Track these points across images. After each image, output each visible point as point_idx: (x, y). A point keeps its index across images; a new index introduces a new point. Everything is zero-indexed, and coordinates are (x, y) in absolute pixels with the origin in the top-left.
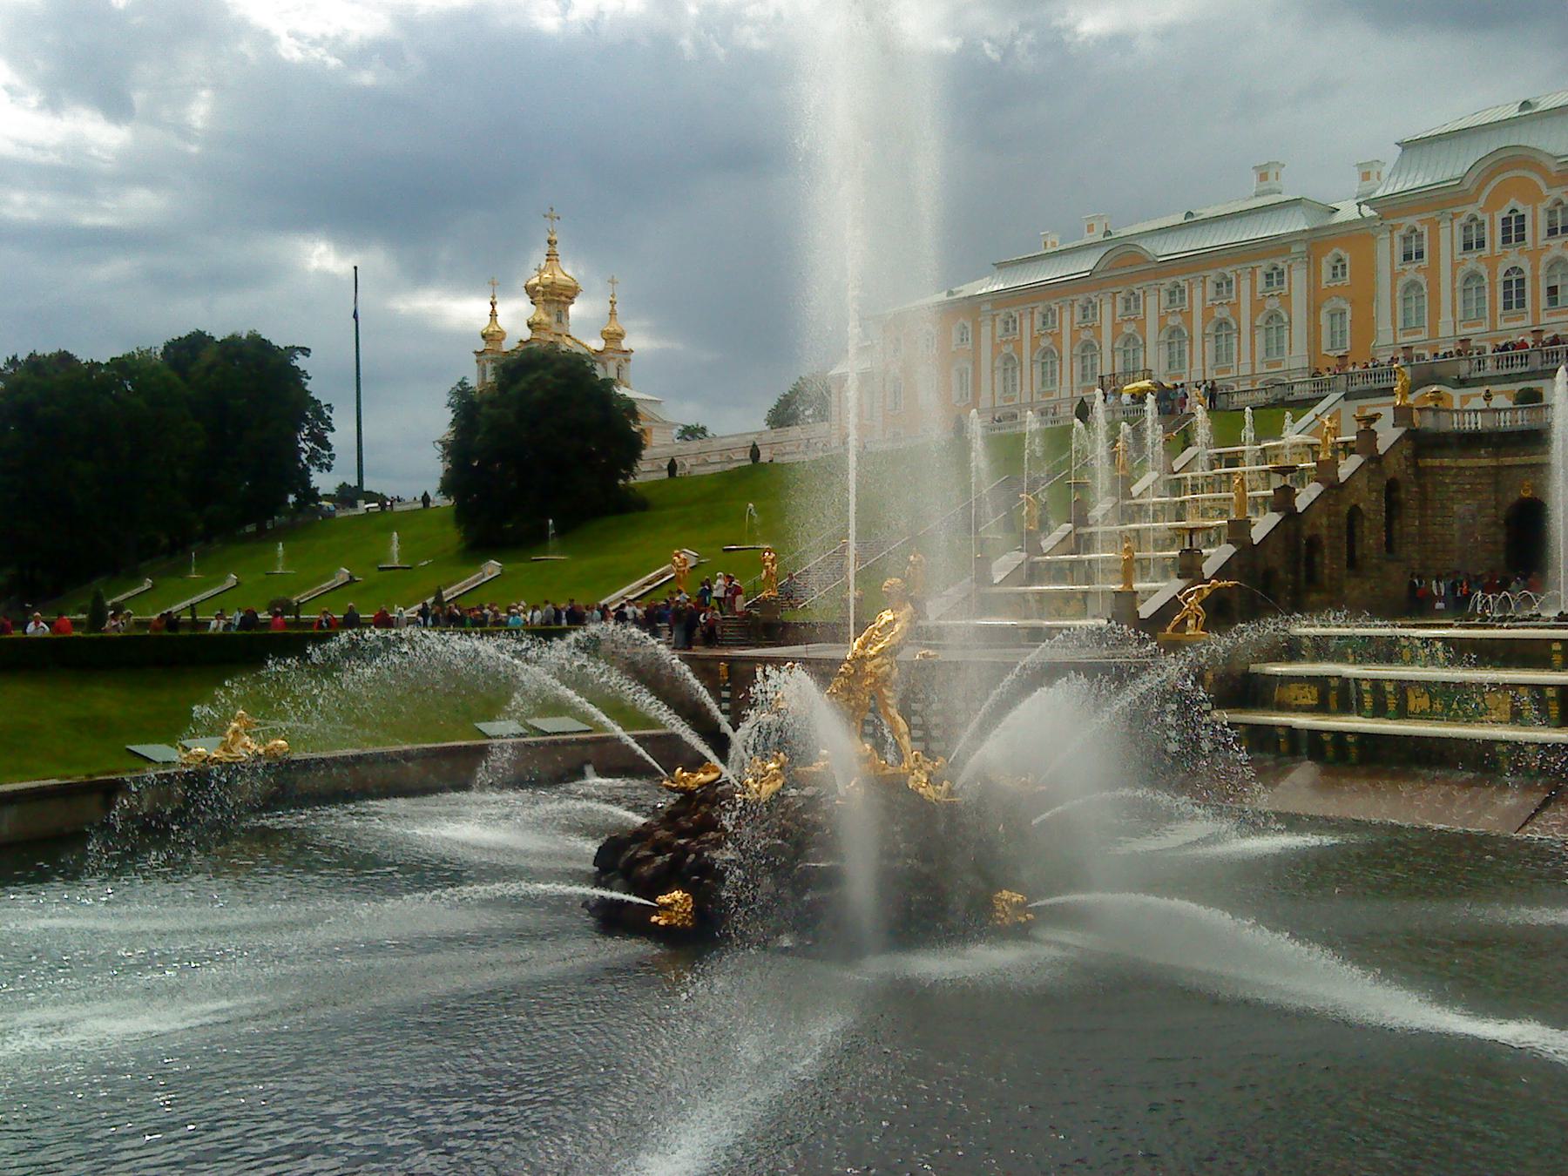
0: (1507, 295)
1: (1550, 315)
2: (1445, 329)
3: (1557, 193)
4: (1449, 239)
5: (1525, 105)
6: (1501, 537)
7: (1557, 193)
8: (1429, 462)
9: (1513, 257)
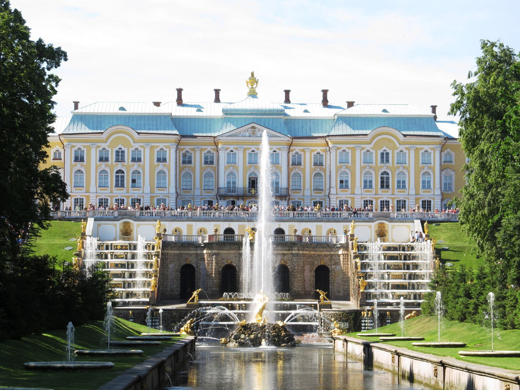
0: (117, 181)
1: (133, 190)
2: (93, 189)
3: (136, 145)
4: (93, 156)
5: (122, 109)
6: (179, 276)
7: (136, 145)
8: (166, 251)
9: (119, 166)
